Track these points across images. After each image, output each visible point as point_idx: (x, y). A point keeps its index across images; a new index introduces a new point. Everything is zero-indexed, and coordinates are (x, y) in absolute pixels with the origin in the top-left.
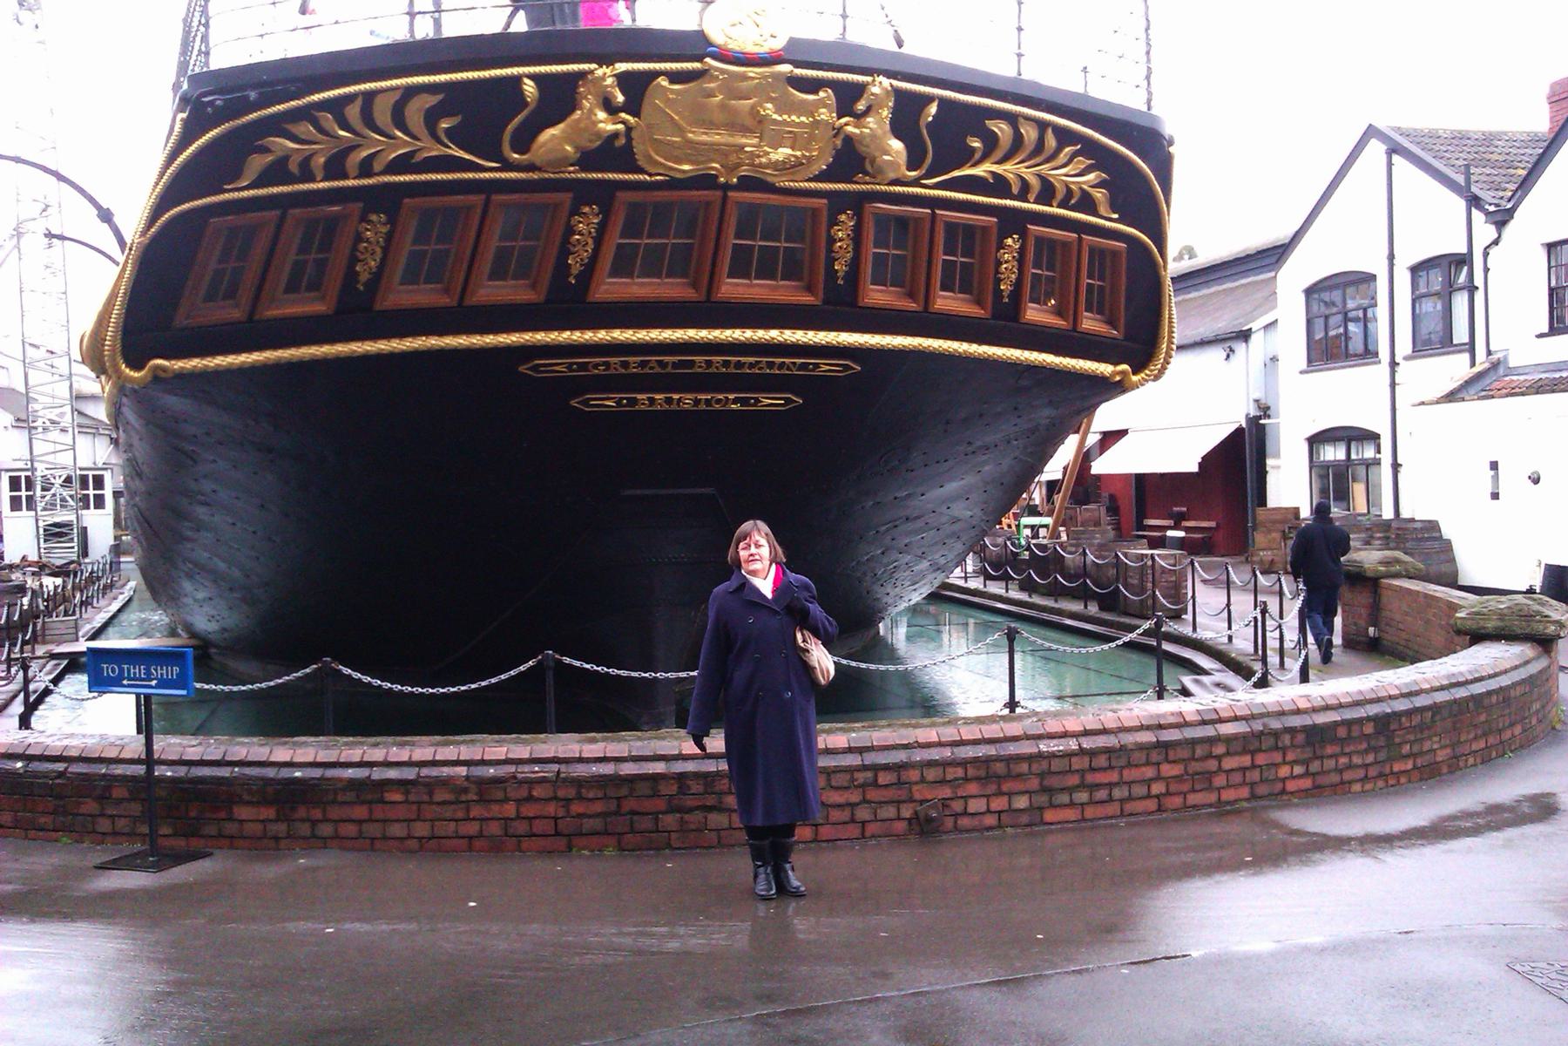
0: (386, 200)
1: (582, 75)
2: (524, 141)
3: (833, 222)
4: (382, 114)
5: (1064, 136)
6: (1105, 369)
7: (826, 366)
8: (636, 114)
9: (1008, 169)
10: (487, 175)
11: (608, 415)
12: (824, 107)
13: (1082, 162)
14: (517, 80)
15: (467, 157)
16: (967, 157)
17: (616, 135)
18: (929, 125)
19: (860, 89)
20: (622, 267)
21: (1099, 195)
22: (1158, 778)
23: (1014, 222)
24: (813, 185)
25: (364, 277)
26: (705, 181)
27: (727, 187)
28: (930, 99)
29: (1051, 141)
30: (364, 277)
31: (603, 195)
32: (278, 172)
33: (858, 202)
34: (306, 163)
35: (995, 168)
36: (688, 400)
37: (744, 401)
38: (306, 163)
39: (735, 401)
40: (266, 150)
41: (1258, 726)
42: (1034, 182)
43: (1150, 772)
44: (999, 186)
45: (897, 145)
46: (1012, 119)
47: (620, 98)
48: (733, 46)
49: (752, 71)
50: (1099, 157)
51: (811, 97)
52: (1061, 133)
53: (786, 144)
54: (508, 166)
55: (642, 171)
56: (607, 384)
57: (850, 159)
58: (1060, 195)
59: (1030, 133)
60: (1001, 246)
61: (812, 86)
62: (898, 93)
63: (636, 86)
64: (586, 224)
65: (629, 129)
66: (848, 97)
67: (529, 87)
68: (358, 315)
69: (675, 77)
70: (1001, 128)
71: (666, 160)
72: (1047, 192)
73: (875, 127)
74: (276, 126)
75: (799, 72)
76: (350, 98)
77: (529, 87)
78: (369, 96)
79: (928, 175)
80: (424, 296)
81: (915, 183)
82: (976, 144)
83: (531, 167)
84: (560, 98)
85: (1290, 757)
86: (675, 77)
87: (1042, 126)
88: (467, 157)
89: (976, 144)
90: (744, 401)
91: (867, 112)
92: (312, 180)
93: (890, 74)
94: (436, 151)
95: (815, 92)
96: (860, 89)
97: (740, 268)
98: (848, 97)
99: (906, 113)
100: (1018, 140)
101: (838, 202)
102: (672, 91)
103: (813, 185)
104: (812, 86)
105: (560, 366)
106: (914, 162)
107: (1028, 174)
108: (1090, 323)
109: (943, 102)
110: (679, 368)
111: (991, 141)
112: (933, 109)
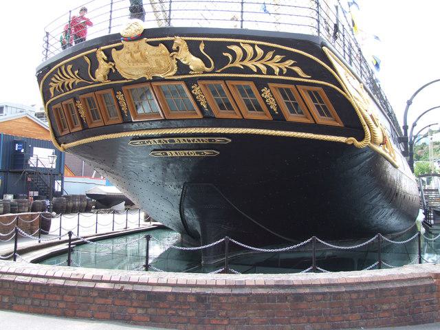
1: (95, 53)
6: (343, 139)
7: (218, 140)
9: (246, 63)
10: (91, 86)
13: (278, 58)
14: (82, 57)
17: (111, 69)
19: (172, 42)
21: (296, 69)
22: (62, 301)
23: (261, 84)
28: (200, 42)
29: (260, 51)
37: (200, 153)
40: (51, 86)
41: (118, 287)
42: (263, 69)
43: (58, 298)
44: (247, 70)
47: (105, 58)
50: (288, 56)
52: (259, 46)
57: (183, 68)
58: (277, 71)
59: (249, 50)
62: (186, 41)
63: (108, 53)
69: (116, 48)
70: (234, 48)
72: (270, 71)
76: (57, 69)
78: (60, 68)
80: (98, 123)
83: (100, 82)
85: (135, 304)
90: (200, 153)
98: (169, 45)
99: (193, 48)
106: (207, 64)
108: (322, 120)
109: (205, 42)
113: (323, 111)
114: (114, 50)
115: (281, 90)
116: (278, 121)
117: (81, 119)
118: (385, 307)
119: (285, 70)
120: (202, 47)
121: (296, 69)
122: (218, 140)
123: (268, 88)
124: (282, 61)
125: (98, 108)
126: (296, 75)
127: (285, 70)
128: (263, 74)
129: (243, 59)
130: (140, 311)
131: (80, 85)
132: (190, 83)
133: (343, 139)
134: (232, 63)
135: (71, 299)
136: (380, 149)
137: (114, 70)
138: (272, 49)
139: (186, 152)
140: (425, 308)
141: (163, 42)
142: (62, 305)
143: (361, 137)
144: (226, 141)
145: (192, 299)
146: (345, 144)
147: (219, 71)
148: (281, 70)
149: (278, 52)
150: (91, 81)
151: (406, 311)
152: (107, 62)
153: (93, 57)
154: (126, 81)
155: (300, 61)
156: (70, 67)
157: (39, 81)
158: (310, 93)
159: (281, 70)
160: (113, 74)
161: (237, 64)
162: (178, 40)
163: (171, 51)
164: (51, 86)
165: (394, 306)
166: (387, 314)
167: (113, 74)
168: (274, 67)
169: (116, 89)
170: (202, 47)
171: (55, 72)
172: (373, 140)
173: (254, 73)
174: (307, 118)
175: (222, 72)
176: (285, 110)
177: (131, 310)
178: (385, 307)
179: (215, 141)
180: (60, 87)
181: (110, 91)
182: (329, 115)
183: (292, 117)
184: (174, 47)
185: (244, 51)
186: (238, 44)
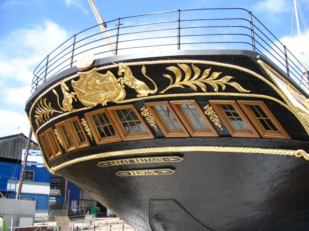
0: (52, 125)
5: (203, 68)
9: (186, 82)
13: (216, 75)
14: (51, 91)
15: (57, 111)
16: (168, 82)
18: (146, 74)
21: (234, 84)
23: (202, 102)
27: (105, 106)
29: (197, 70)
35: (181, 83)
42: (201, 85)
44: (187, 89)
46: (175, 65)
50: (225, 72)
51: (105, 75)
52: (196, 65)
54: (64, 112)
55: (85, 107)
63: (68, 83)
67: (54, 91)
72: (210, 88)
73: (129, 80)
76: (37, 103)
77: (54, 91)
79: (160, 90)
81: (157, 94)
82: (168, 76)
87: (189, 65)
88: (57, 111)
89: (168, 76)
102: (76, 83)
104: (104, 72)
107: (198, 83)
109: (146, 66)
114: (73, 81)
117: (60, 144)
119: (224, 87)
120: (144, 70)
121: (234, 84)
124: (219, 77)
125: (70, 135)
127: (224, 87)
128: (202, 92)
129: (182, 80)
131: (55, 114)
132: (138, 105)
134: (173, 83)
137: (76, 100)
138: (208, 66)
139: (146, 171)
141: (110, 69)
144: (178, 160)
147: (163, 92)
148: (220, 87)
149: (215, 69)
150: (62, 111)
152: (70, 92)
153: (58, 89)
154: (85, 108)
155: (238, 77)
156: (45, 100)
159: (220, 87)
160: (77, 104)
161: (178, 84)
163: (117, 77)
164: (36, 118)
168: (212, 84)
169: (81, 115)
170: (144, 70)
173: (193, 91)
175: (165, 93)
181: (76, 118)
184: (119, 74)
185: (182, 71)
186: (175, 65)
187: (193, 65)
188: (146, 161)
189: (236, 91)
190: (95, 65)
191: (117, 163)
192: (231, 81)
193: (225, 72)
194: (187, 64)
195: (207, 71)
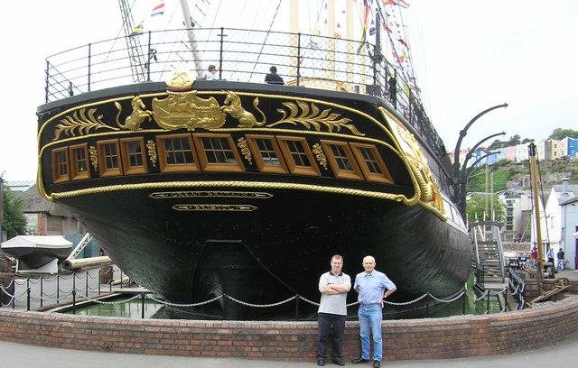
0: (91, 141)
1: (131, 99)
2: (123, 121)
3: (236, 142)
4: (82, 113)
6: (391, 196)
7: (258, 195)
8: (151, 110)
9: (302, 120)
11: (184, 212)
12: (214, 104)
14: (114, 102)
17: (147, 118)
19: (225, 96)
20: (171, 161)
21: (350, 127)
22: (190, 344)
23: (313, 140)
24: (222, 130)
25: (95, 166)
26: (184, 130)
27: (192, 132)
29: (315, 109)
30: (95, 166)
31: (148, 137)
32: (63, 135)
33: (242, 134)
34: (69, 131)
36: (213, 207)
37: (235, 208)
38: (69, 131)
39: (231, 207)
42: (315, 124)
43: (187, 342)
45: (247, 113)
46: (294, 102)
47: (144, 106)
48: (174, 86)
49: (183, 94)
50: (344, 114)
52: (316, 104)
53: (207, 117)
54: (122, 130)
56: (185, 201)
57: (231, 121)
58: (331, 128)
59: (304, 107)
60: (312, 149)
61: (207, 97)
62: (240, 96)
63: (148, 102)
64: (151, 145)
65: (151, 116)
66: (221, 99)
67: (117, 105)
68: (96, 179)
69: (159, 98)
70: (290, 105)
71: (166, 125)
72: (324, 128)
74: (58, 121)
75: (199, 92)
76: (73, 112)
78: (78, 111)
80: (115, 172)
81: (263, 126)
83: (128, 130)
84: (127, 107)
85: (250, 344)
86: (159, 98)
87: (309, 103)
90: (235, 208)
91: (230, 104)
92: (72, 136)
93: (234, 90)
94: (100, 126)
95: (208, 98)
96: (225, 96)
97: (211, 158)
98: (221, 99)
99: (247, 103)
100: (300, 111)
101: (236, 135)
103: (222, 130)
104: (207, 97)
105: (162, 195)
106: (259, 118)
107: (312, 121)
108: (374, 177)
109: (259, 98)
110: (203, 196)
111: (289, 111)
112: (257, 101)
113: (374, 168)
114: (156, 100)
115: (333, 147)
116: (327, 177)
118: (435, 344)
119: (339, 127)
121: (350, 127)
122: (258, 195)
123: (320, 144)
125: (118, 155)
126: (349, 132)
130: (254, 349)
133: (391, 196)
135: (197, 342)
136: (429, 205)
138: (328, 107)
140: (464, 346)
142: (189, 348)
143: (411, 193)
144: (267, 196)
145: (295, 339)
146: (394, 201)
149: (334, 110)
151: (449, 348)
156: (92, 111)
157: (41, 122)
158: (362, 149)
162: (231, 94)
165: (441, 344)
166: (436, 350)
167: (148, 123)
171: (71, 114)
172: (423, 198)
174: (356, 174)
175: (272, 127)
176: (335, 165)
177: (248, 349)
178: (435, 344)
179: (255, 195)
180: (72, 131)
182: (379, 172)
183: (342, 174)
185: (299, 108)
187: (313, 105)
188: (214, 194)
189: (349, 132)
190: (194, 87)
191: (175, 195)
192: (348, 123)
193: (344, 114)
194: (307, 102)
195: (325, 112)
